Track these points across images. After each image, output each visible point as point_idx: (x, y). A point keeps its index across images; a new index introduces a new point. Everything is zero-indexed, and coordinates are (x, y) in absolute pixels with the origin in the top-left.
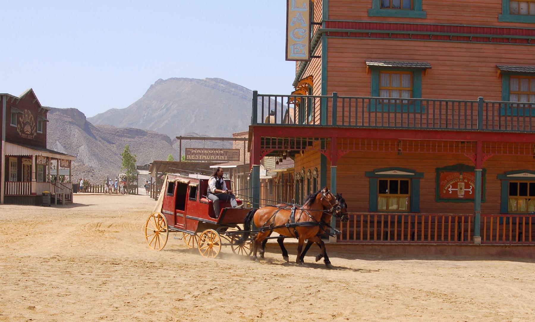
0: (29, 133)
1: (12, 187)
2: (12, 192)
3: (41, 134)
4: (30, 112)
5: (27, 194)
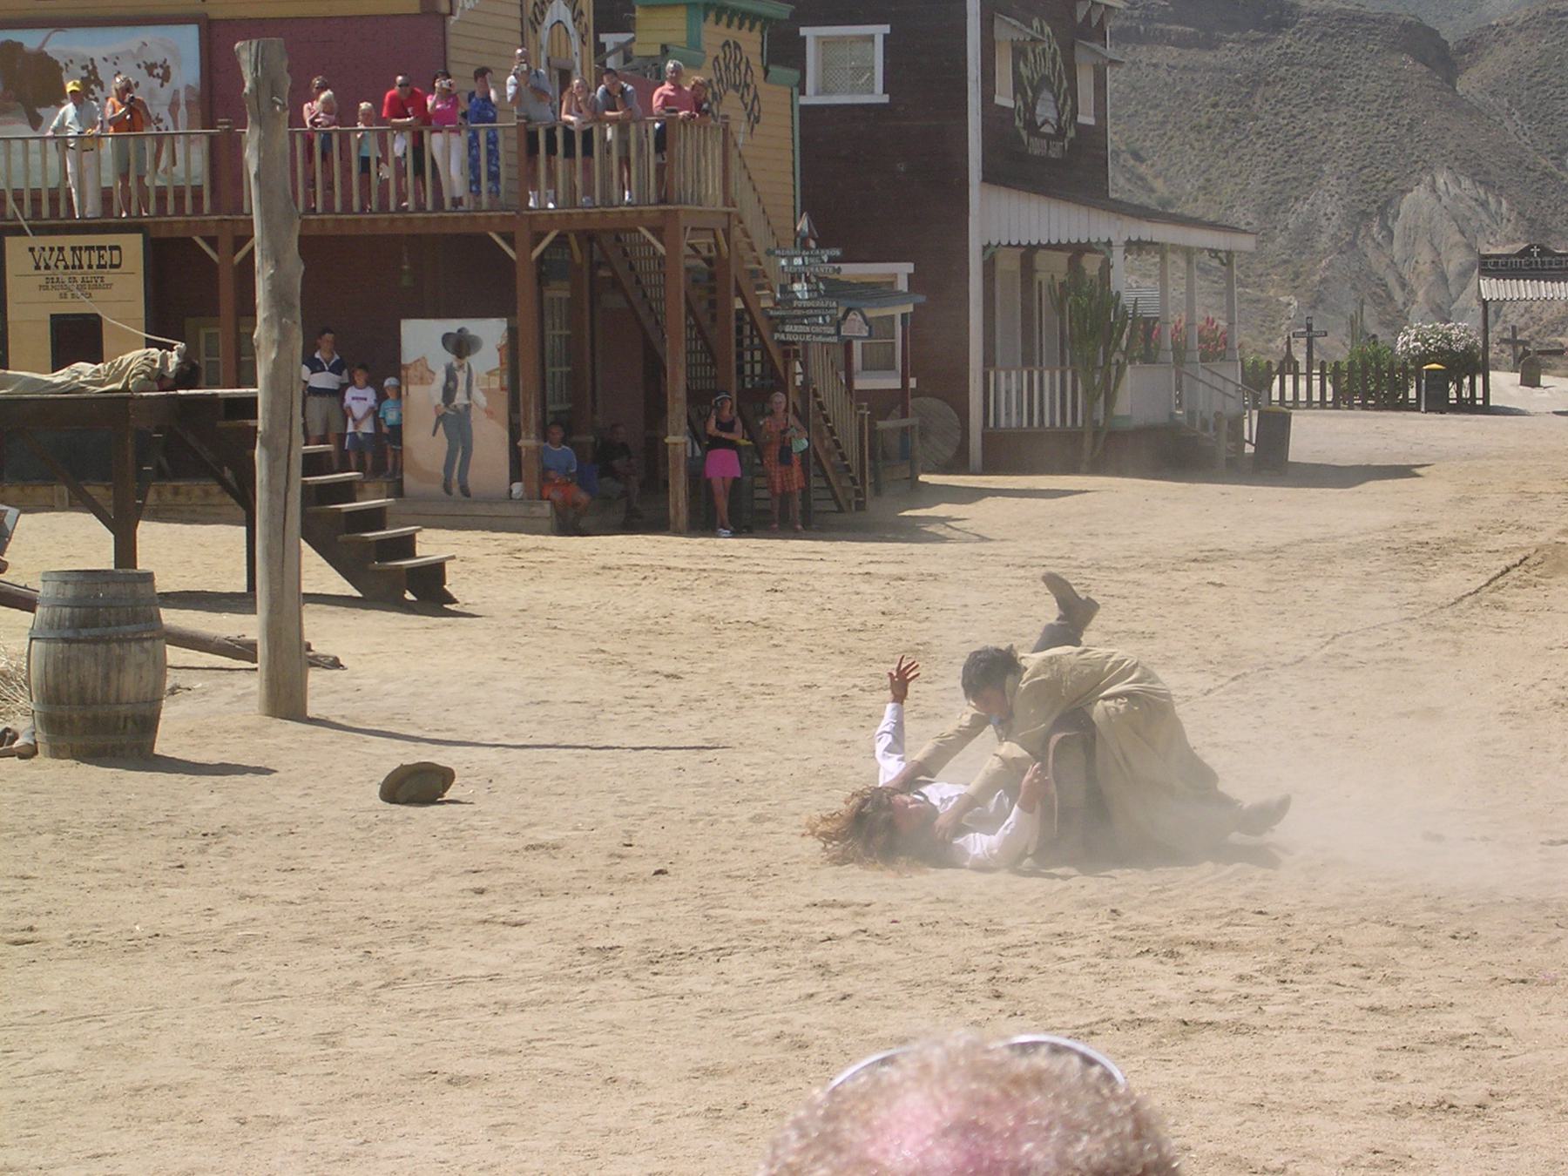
0: (1052, 132)
1: (1008, 392)
2: (1008, 414)
3: (1090, 126)
4: (1048, 29)
5: (1058, 423)
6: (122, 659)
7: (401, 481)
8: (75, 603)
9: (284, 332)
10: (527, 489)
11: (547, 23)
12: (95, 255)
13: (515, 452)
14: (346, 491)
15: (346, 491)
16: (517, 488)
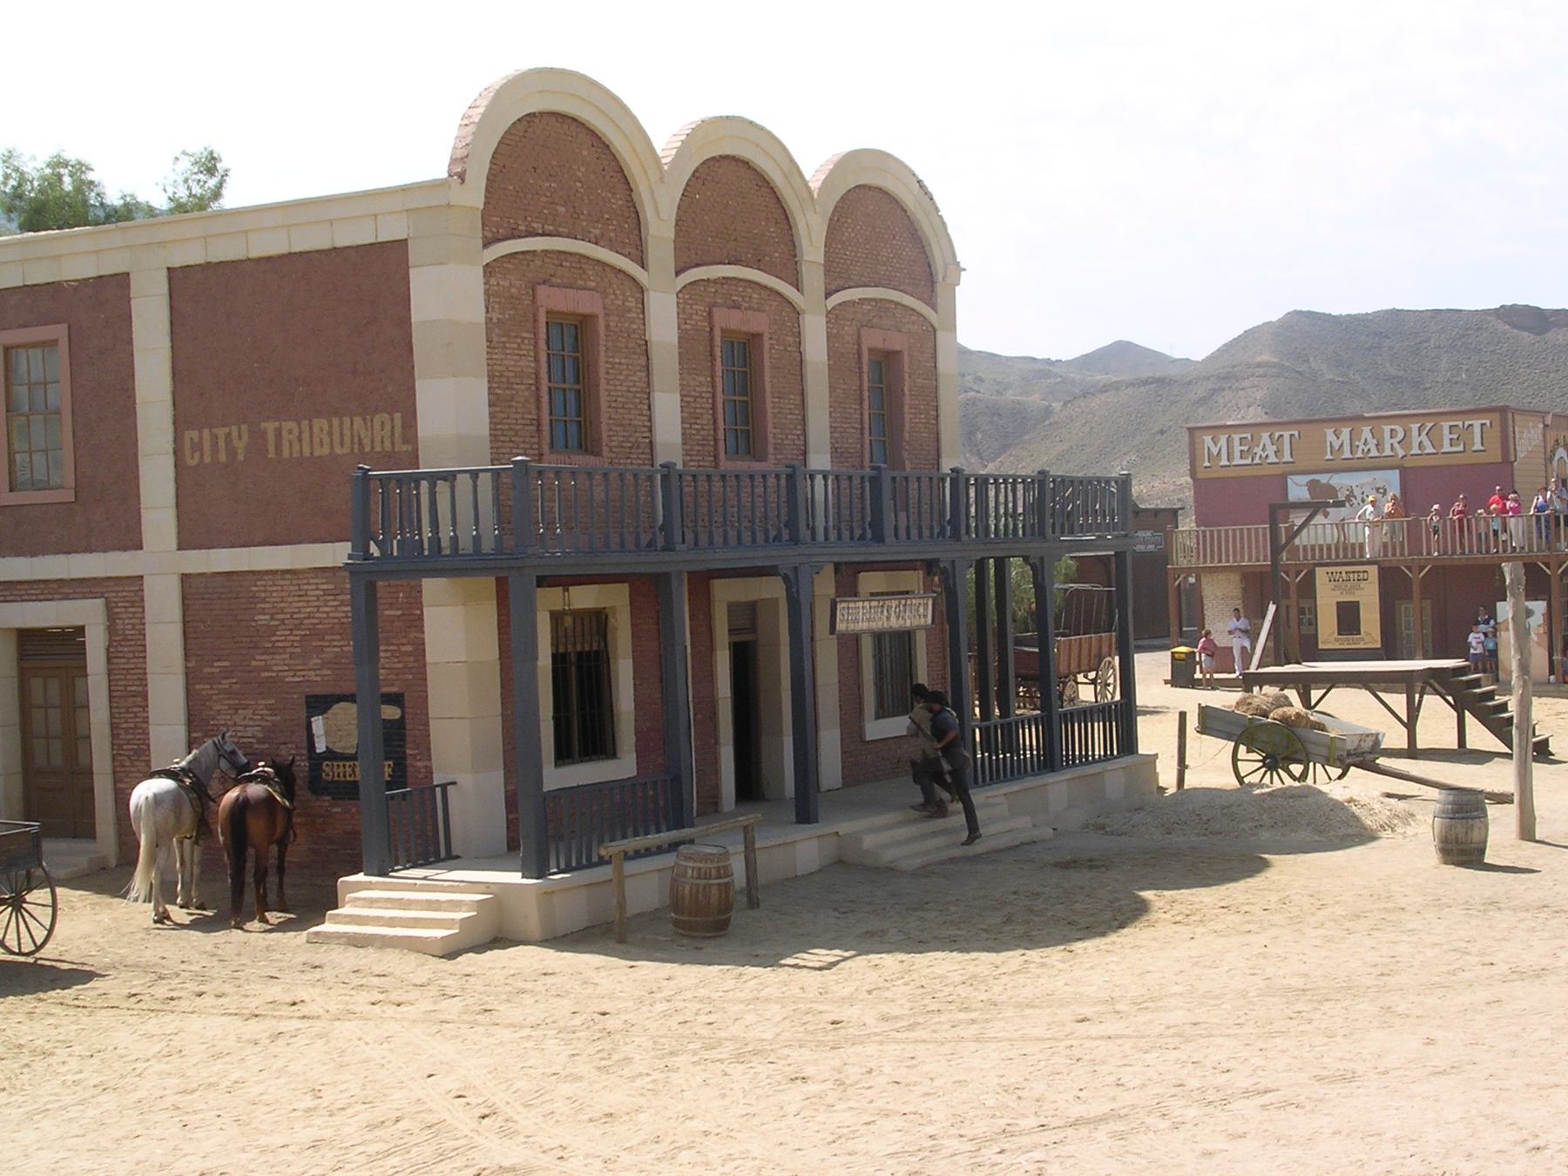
6: (1472, 825)
7: (1498, 675)
8: (1453, 803)
9: (1525, 682)
10: (1557, 679)
11: (1556, 459)
12: (1356, 575)
13: (1551, 662)
14: (1476, 683)
15: (1476, 683)
16: (1552, 677)
